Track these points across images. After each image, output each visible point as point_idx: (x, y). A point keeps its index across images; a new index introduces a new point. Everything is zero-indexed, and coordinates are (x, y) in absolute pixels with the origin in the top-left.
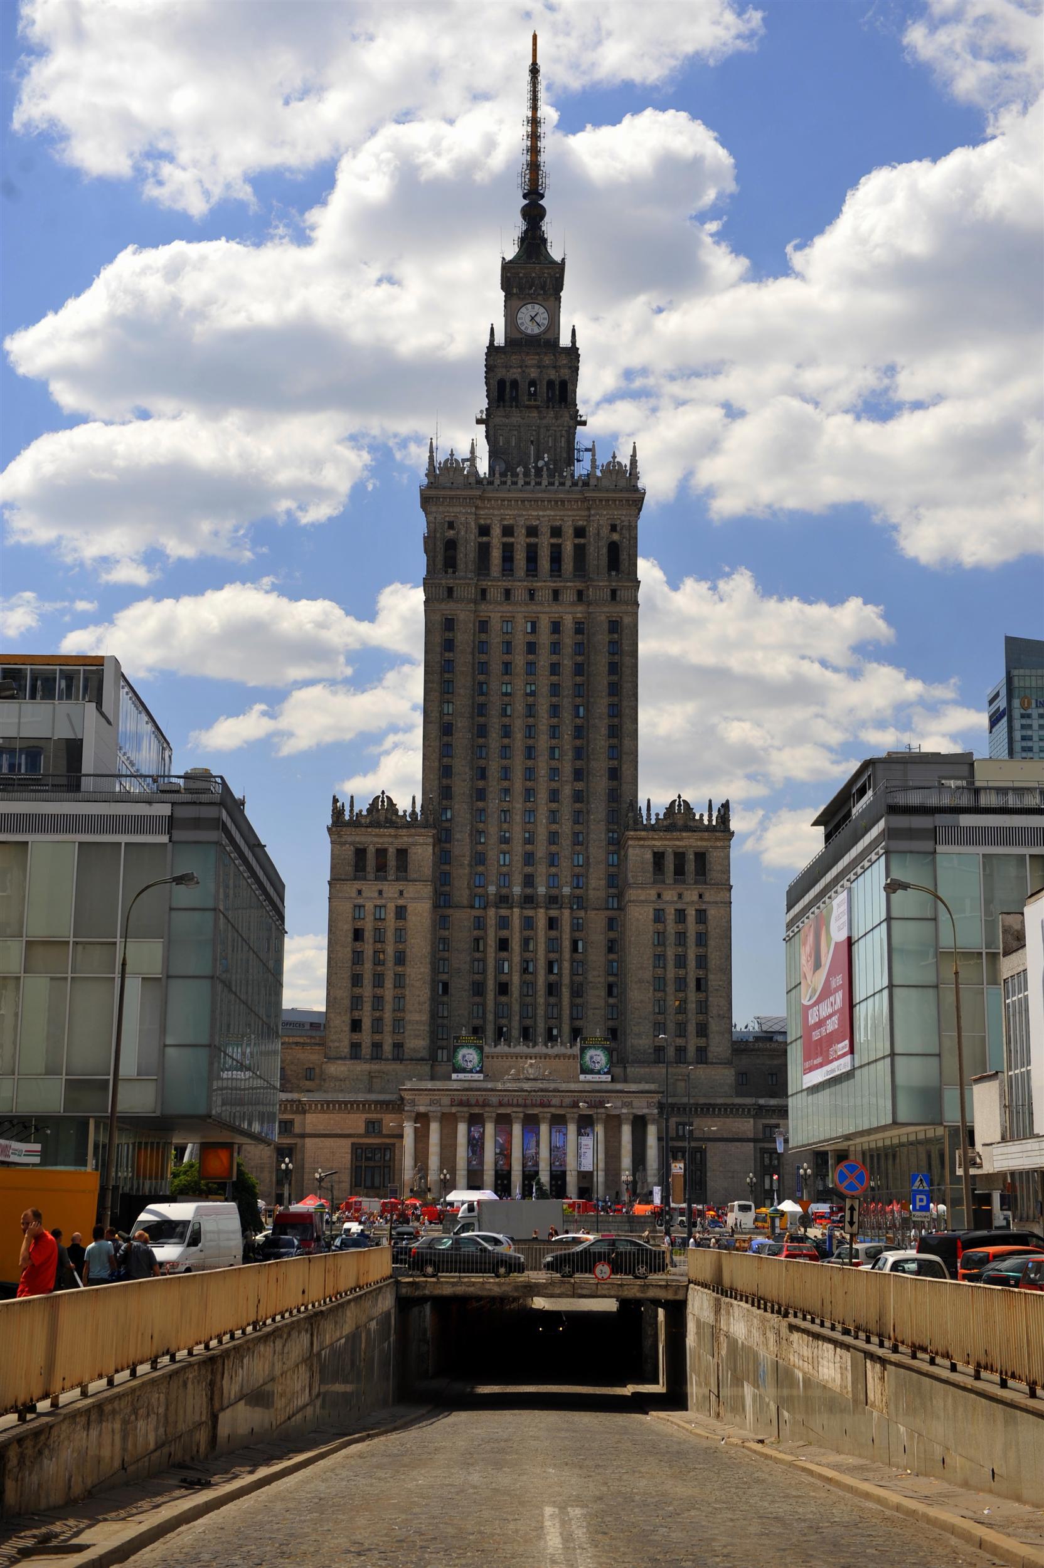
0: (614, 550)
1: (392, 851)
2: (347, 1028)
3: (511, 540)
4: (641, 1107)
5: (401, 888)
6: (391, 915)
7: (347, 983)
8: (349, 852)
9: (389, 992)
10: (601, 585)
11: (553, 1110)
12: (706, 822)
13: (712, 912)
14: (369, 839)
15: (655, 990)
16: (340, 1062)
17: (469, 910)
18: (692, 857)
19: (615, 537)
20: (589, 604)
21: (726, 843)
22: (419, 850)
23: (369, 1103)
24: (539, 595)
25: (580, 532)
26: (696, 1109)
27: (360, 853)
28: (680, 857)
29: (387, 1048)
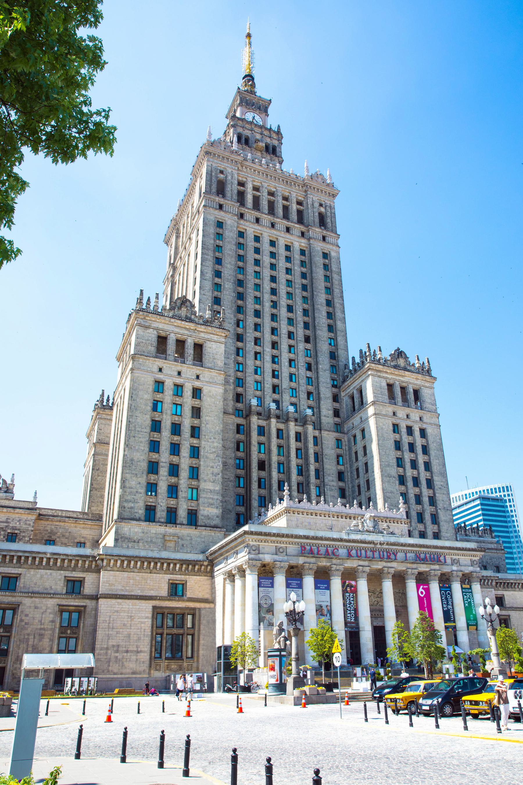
2: (143, 491)
3: (258, 194)
5: (198, 372)
6: (188, 392)
7: (145, 447)
10: (316, 231)
13: (430, 431)
16: (135, 522)
17: (233, 417)
18: (412, 390)
22: (214, 345)
23: (175, 562)
24: (277, 226)
25: (299, 203)
27: (162, 340)
28: (403, 389)
29: (182, 514)
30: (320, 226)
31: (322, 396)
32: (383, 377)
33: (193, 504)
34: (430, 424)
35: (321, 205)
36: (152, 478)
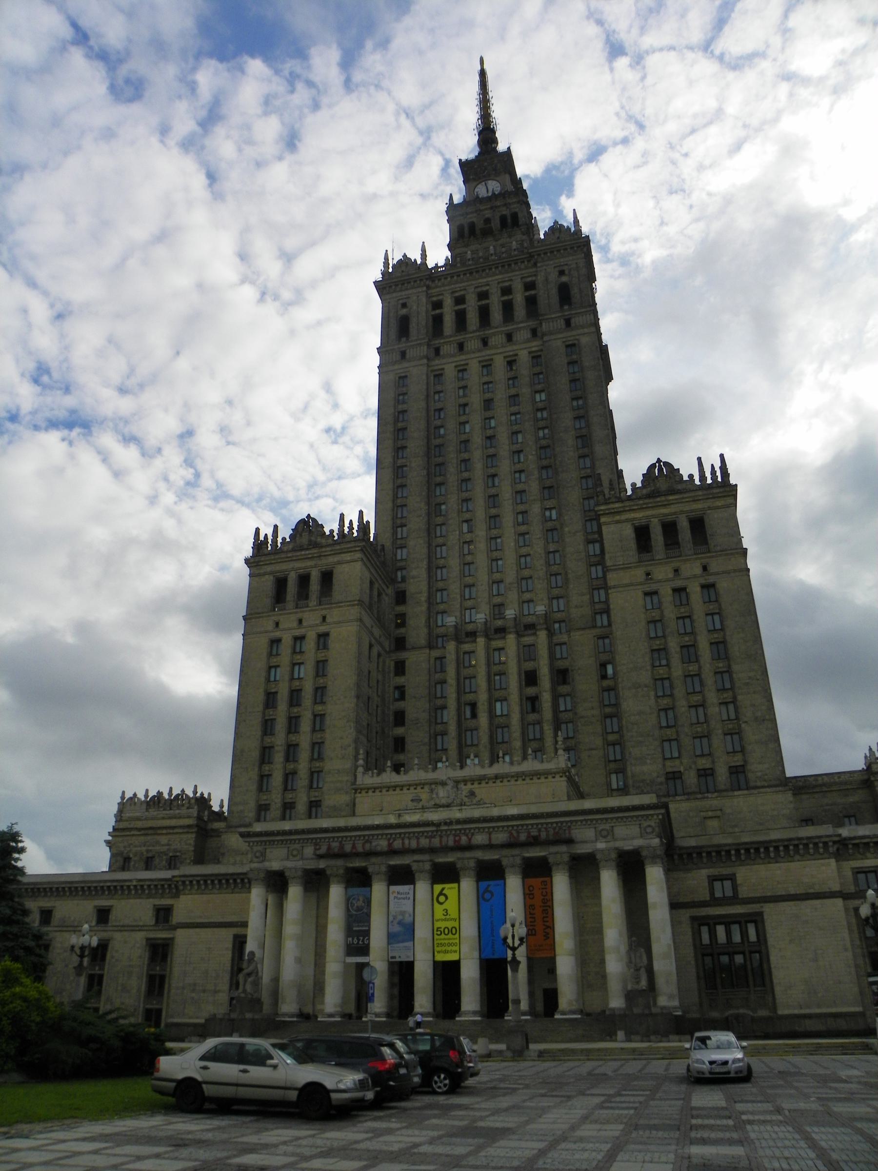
0: (565, 294)
1: (315, 576)
2: (254, 787)
3: (462, 307)
4: (630, 837)
5: (324, 612)
7: (257, 732)
8: (268, 582)
9: (304, 738)
11: (479, 854)
12: (697, 482)
13: (723, 585)
14: (291, 565)
15: (657, 697)
19: (564, 279)
20: (544, 335)
21: (730, 500)
22: (345, 568)
24: (492, 341)
25: (530, 286)
26: (738, 851)
30: (562, 306)
31: (570, 576)
32: (627, 520)
33: (317, 794)
34: (724, 572)
35: (562, 273)
36: (267, 768)
